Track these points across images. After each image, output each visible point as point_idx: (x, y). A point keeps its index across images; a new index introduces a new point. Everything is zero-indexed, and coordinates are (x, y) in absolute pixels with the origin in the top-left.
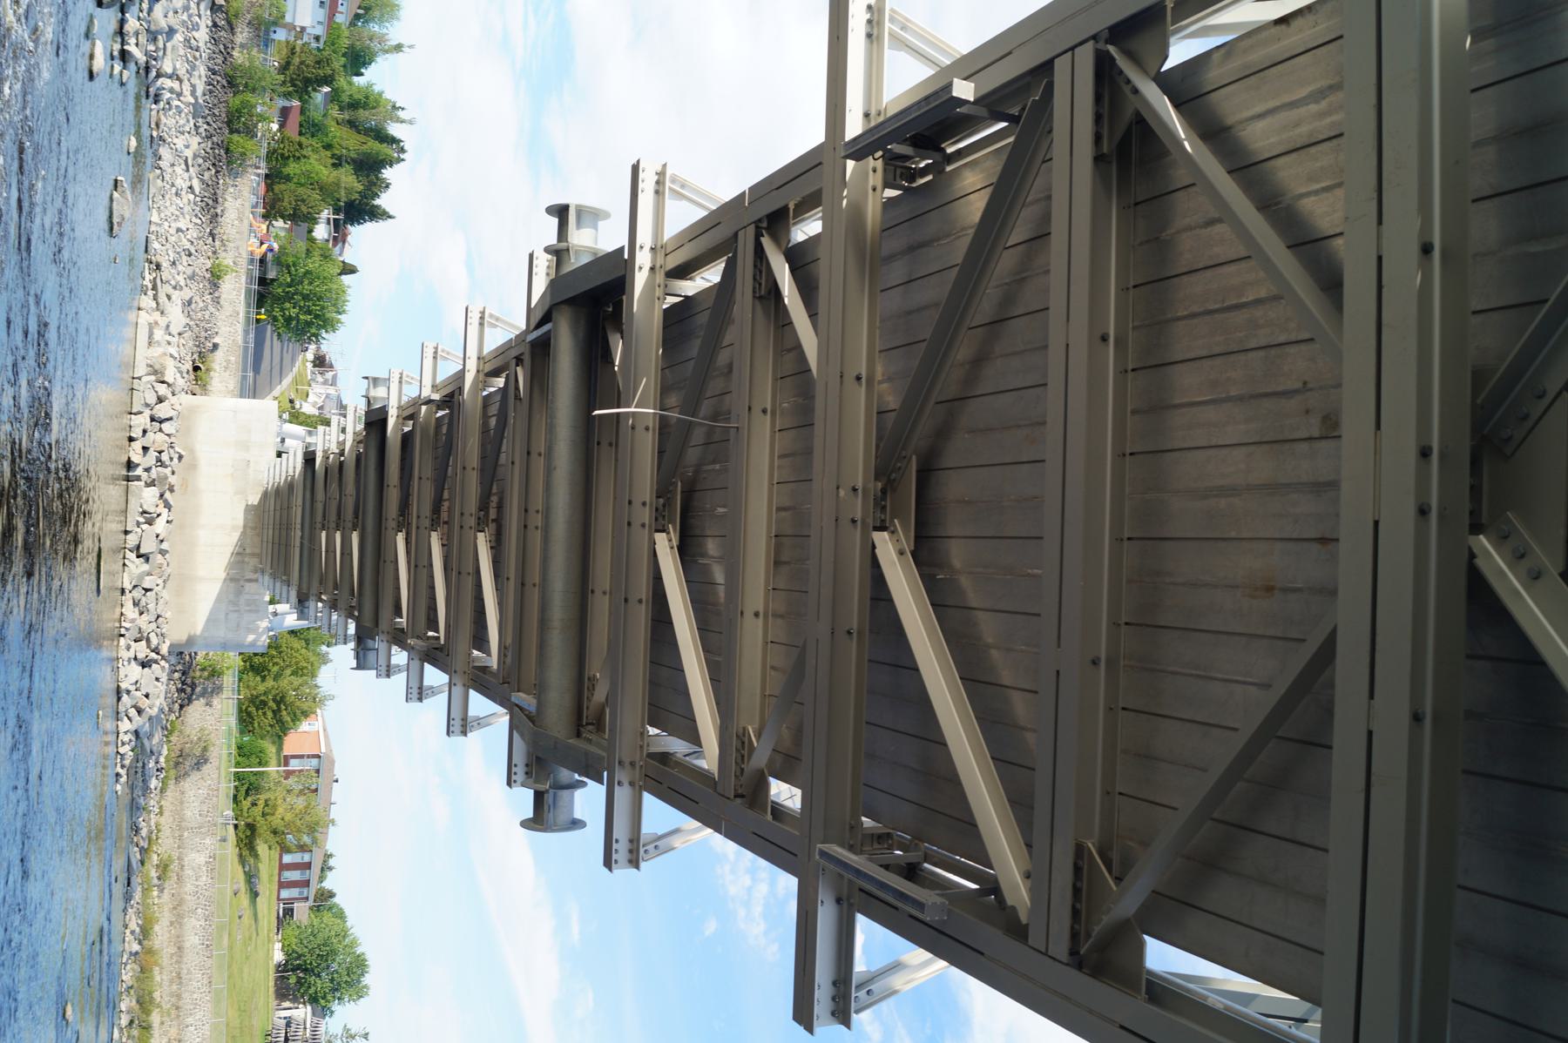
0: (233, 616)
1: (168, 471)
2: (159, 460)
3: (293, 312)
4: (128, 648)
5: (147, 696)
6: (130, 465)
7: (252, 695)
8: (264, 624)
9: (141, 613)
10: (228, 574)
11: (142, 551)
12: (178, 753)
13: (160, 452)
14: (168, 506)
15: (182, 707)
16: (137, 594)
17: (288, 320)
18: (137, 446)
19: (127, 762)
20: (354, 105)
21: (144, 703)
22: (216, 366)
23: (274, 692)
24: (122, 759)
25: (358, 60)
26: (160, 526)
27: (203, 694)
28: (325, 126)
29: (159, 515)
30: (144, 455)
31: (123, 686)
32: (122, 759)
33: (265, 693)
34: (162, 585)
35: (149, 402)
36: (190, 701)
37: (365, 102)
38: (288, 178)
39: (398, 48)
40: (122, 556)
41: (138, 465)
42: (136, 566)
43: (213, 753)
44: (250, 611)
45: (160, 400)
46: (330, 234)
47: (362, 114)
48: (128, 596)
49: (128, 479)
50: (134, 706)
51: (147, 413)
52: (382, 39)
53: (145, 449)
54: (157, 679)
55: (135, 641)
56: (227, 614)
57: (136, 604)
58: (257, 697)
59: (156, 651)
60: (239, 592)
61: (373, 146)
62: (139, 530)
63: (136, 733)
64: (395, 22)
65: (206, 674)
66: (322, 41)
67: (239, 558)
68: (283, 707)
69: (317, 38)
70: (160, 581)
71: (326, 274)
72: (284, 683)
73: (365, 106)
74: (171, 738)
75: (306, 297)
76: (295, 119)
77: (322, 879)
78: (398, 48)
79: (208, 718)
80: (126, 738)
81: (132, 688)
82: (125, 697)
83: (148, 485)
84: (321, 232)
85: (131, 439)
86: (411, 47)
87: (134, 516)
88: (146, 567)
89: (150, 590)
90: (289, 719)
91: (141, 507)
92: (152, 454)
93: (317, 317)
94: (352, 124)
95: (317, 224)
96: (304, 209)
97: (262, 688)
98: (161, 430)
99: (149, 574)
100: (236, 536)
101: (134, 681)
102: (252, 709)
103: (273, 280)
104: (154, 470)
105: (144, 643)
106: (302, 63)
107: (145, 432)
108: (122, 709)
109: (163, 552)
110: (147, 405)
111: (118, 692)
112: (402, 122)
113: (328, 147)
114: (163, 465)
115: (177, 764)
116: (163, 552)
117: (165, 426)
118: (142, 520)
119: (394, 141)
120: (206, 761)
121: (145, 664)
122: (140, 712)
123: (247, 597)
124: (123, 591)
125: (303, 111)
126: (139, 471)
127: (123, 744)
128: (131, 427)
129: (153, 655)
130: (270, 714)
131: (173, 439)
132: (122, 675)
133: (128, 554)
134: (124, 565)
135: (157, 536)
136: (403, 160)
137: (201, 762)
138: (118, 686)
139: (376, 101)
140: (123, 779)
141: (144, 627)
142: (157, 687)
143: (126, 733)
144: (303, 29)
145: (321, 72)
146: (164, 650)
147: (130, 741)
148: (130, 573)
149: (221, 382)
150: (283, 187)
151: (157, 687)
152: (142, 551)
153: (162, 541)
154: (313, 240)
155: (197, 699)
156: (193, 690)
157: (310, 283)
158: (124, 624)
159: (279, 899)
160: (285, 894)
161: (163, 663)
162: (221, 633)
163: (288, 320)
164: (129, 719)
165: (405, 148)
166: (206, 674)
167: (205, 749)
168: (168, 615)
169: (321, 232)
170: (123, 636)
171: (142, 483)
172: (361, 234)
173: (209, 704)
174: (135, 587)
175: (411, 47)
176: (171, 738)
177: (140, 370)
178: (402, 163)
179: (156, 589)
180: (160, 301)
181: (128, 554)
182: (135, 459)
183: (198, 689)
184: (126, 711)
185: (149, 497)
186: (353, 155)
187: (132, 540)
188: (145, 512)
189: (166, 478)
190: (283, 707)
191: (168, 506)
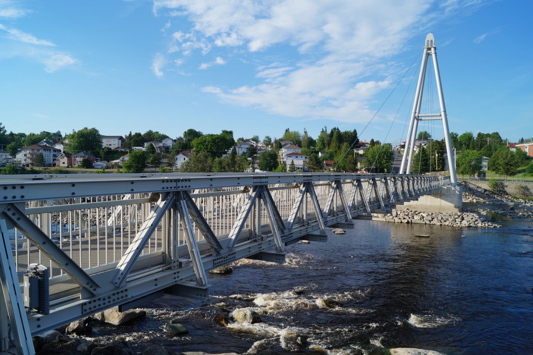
0: (451, 196)
1: (410, 213)
2: (407, 215)
3: (384, 161)
4: (457, 223)
5: (472, 219)
6: (408, 223)
7: (505, 173)
8: (453, 188)
9: (448, 220)
10: (439, 198)
11: (431, 219)
12: (523, 195)
13: (405, 215)
15: (507, 194)
16: (442, 221)
17: (387, 162)
18: (403, 221)
19: (491, 224)
20: (323, 144)
21: (474, 220)
23: (504, 166)
24: (489, 226)
25: (311, 142)
26: (424, 215)
27: (503, 187)
28: (331, 152)
29: (422, 215)
30: (406, 219)
31: (467, 225)
32: (489, 226)
33: (504, 169)
34: (441, 215)
35: (392, 218)
36: (505, 192)
37: (322, 139)
38: (344, 166)
39: (306, 132)
40: (432, 226)
41: (408, 220)
42: (435, 222)
43: (524, 184)
44: (450, 192)
46: (362, 149)
47: (326, 142)
48: (443, 223)
49: (412, 223)
50: (475, 222)
51: (395, 218)
52: (304, 137)
53: (404, 219)
54: (468, 216)
55: (456, 221)
56: (451, 198)
57: (445, 221)
58: (505, 171)
59: (459, 216)
60: (444, 195)
61: (334, 138)
63: (483, 222)
64: (299, 133)
65: (496, 187)
66: (306, 156)
67: (435, 195)
68: (510, 163)
69: (306, 158)
70: (440, 215)
71: (372, 152)
72: (501, 163)
73: (323, 141)
74: (518, 197)
75: (379, 157)
76: (329, 162)
78: (306, 132)
79: (511, 186)
80: (483, 224)
81: (469, 223)
82: (471, 225)
83: (413, 218)
84: (361, 152)
85: (401, 222)
86: (305, 129)
87: (421, 222)
88: (435, 219)
89: (442, 217)
90: (514, 161)
91: (419, 220)
92: (406, 217)
93: (385, 154)
94: (329, 144)
95: (358, 153)
96: (352, 161)
97: (502, 170)
98: (399, 215)
99: (438, 218)
101: (467, 222)
102: (510, 173)
103: (376, 167)
104: (410, 217)
105: (456, 219)
106: (312, 164)
107: (400, 219)
108: (474, 226)
109: (432, 214)
110: (393, 218)
111: (469, 227)
112: (326, 130)
113: (336, 152)
114: (408, 214)
115: (527, 196)
116: (432, 214)
117: (398, 213)
118: (422, 220)
119: (332, 132)
120: (526, 187)
121: (463, 219)
122: (476, 221)
123: (445, 193)
124: (441, 225)
125: (327, 160)
126: (410, 220)
127: (485, 225)
128: (398, 222)
129: (460, 217)
130: (512, 167)
131: (402, 211)
132: (464, 226)
133: (431, 223)
134: (434, 224)
135: (427, 216)
136: (338, 128)
137: (526, 188)
138: (467, 227)
139: (321, 138)
140: (496, 225)
141: (452, 219)
142: (470, 216)
143: (482, 224)
144: (304, 162)
145: (314, 159)
146: (459, 214)
147: (485, 223)
148: (436, 223)
150: (347, 167)
151: (470, 216)
152: (431, 219)
153: (429, 214)
154: (364, 154)
155: (504, 190)
156: (502, 191)
157: (375, 156)
158: (450, 225)
161: (463, 214)
162: (456, 199)
163: (387, 162)
164: (478, 223)
165: (334, 128)
166: (496, 187)
167: (522, 187)
168: (450, 212)
169: (361, 152)
170: (453, 226)
171: (413, 219)
172: (362, 138)
173: (506, 186)
174: (441, 222)
175: (305, 129)
176: (518, 197)
178: (339, 128)
179: (442, 216)
181: (431, 223)
182: (406, 221)
183: (501, 189)
184: (475, 224)
185: (416, 217)
186: (337, 144)
187: (428, 222)
188: (421, 219)
189: (412, 213)
190: (510, 163)
191: (419, 213)
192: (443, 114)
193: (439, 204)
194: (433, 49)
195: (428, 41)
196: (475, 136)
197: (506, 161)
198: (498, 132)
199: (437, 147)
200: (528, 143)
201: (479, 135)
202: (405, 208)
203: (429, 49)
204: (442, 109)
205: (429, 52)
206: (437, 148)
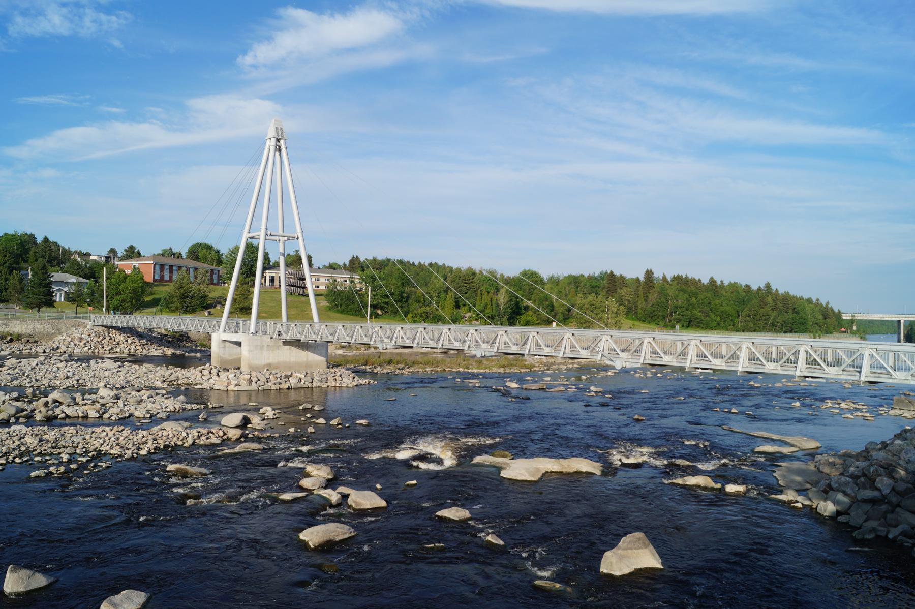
0: (319, 348)
6: (288, 389)
14: (292, 374)
18: (281, 386)
22: (6, 330)
36: (188, 337)
45: (259, 380)
53: (280, 384)
62: (306, 383)
77: (179, 256)
87: (299, 385)
100: (293, 348)
107: (275, 384)
118: (303, 383)
149: (16, 327)
159: (217, 284)
160: (215, 282)
177: (254, 386)
180: (175, 379)
187: (310, 385)
191: (292, 374)
192: (300, 235)
193: (305, 359)
194: (282, 142)
195: (277, 128)
196: (39, 240)
197: (183, 291)
198: (33, 233)
199: (7, 258)
200: (138, 261)
201: (46, 240)
202: (264, 369)
203: (278, 140)
204: (299, 230)
205: (278, 143)
206: (8, 261)
